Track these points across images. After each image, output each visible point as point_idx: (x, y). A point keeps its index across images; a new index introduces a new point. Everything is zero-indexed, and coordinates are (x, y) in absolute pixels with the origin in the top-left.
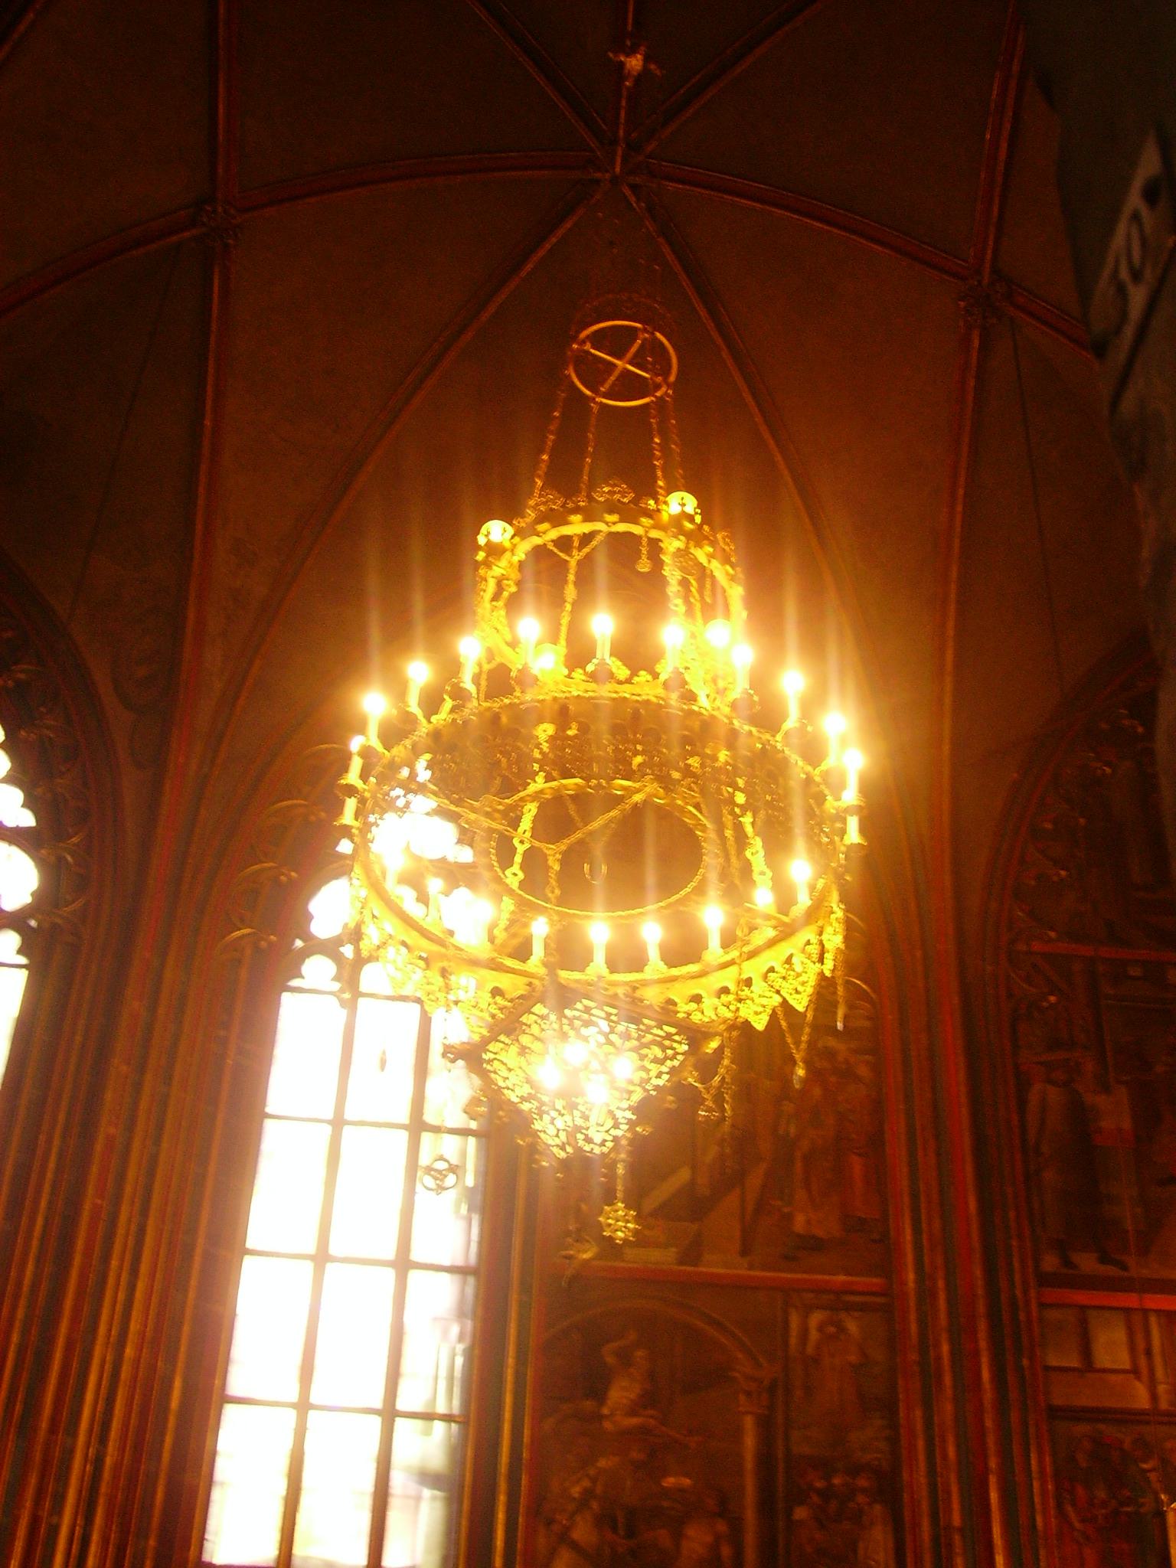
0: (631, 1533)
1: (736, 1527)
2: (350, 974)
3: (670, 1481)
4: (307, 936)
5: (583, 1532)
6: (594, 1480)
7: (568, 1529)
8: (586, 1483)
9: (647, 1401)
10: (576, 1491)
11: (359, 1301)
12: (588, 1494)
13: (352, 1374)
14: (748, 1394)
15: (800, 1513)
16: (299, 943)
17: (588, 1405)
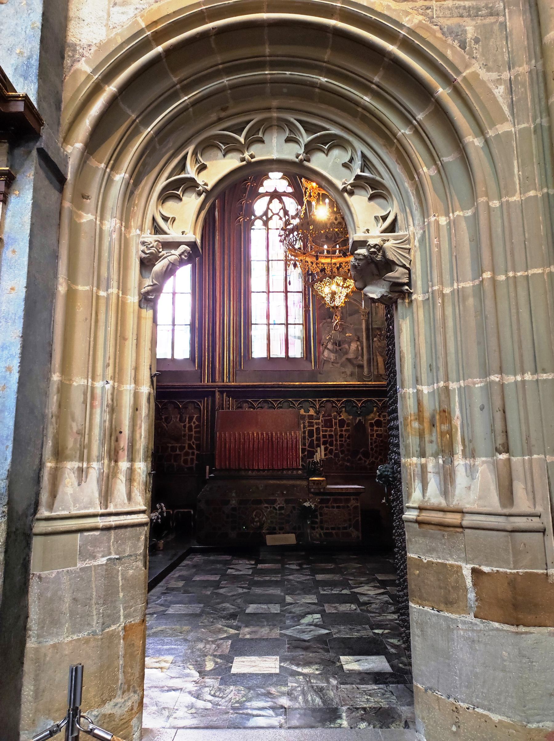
0: (340, 346)
1: (362, 343)
2: (266, 223)
3: (347, 335)
4: (255, 216)
5: (330, 346)
6: (331, 336)
7: (327, 346)
8: (330, 336)
9: (341, 319)
10: (328, 338)
11: (278, 300)
12: (330, 339)
13: (278, 315)
14: (363, 315)
15: (375, 339)
16: (253, 217)
17: (329, 320)
